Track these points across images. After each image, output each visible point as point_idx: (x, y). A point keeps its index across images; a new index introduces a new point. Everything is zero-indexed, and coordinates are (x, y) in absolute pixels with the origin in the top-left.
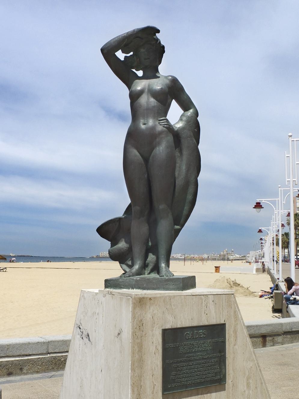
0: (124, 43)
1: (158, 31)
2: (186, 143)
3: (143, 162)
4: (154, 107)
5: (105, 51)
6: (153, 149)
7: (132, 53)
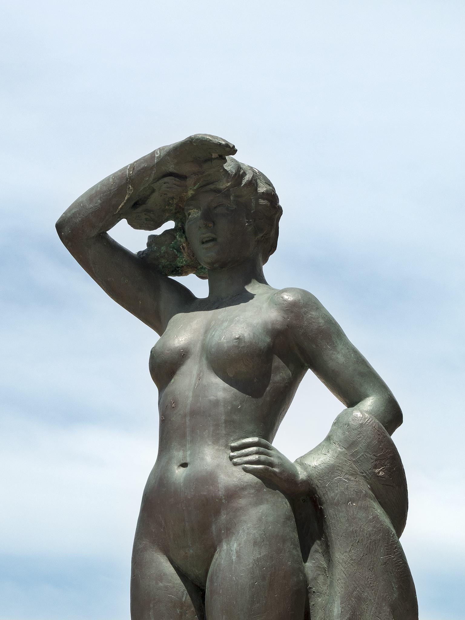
0: (136, 192)
1: (233, 150)
2: (351, 515)
3: (186, 598)
4: (216, 403)
5: (67, 230)
6: (210, 550)
7: (170, 225)
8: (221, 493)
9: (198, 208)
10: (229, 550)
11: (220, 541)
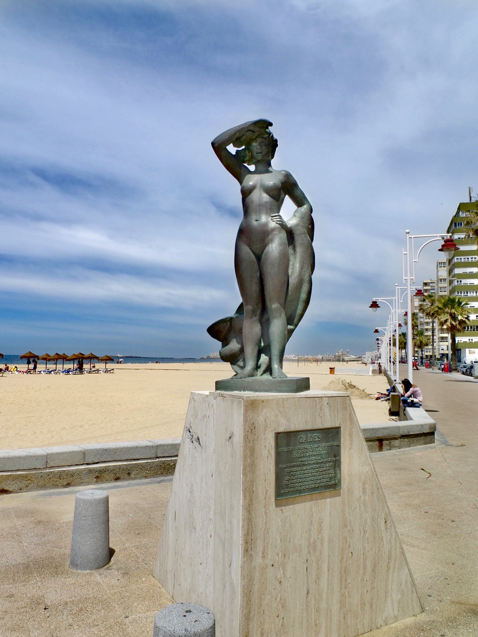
0: (237, 137)
1: (271, 124)
2: (300, 239)
3: (255, 260)
4: (266, 202)
5: (216, 145)
6: (265, 246)
7: (243, 147)
8: (270, 229)
9: (256, 142)
10: (272, 247)
11: (268, 244)
